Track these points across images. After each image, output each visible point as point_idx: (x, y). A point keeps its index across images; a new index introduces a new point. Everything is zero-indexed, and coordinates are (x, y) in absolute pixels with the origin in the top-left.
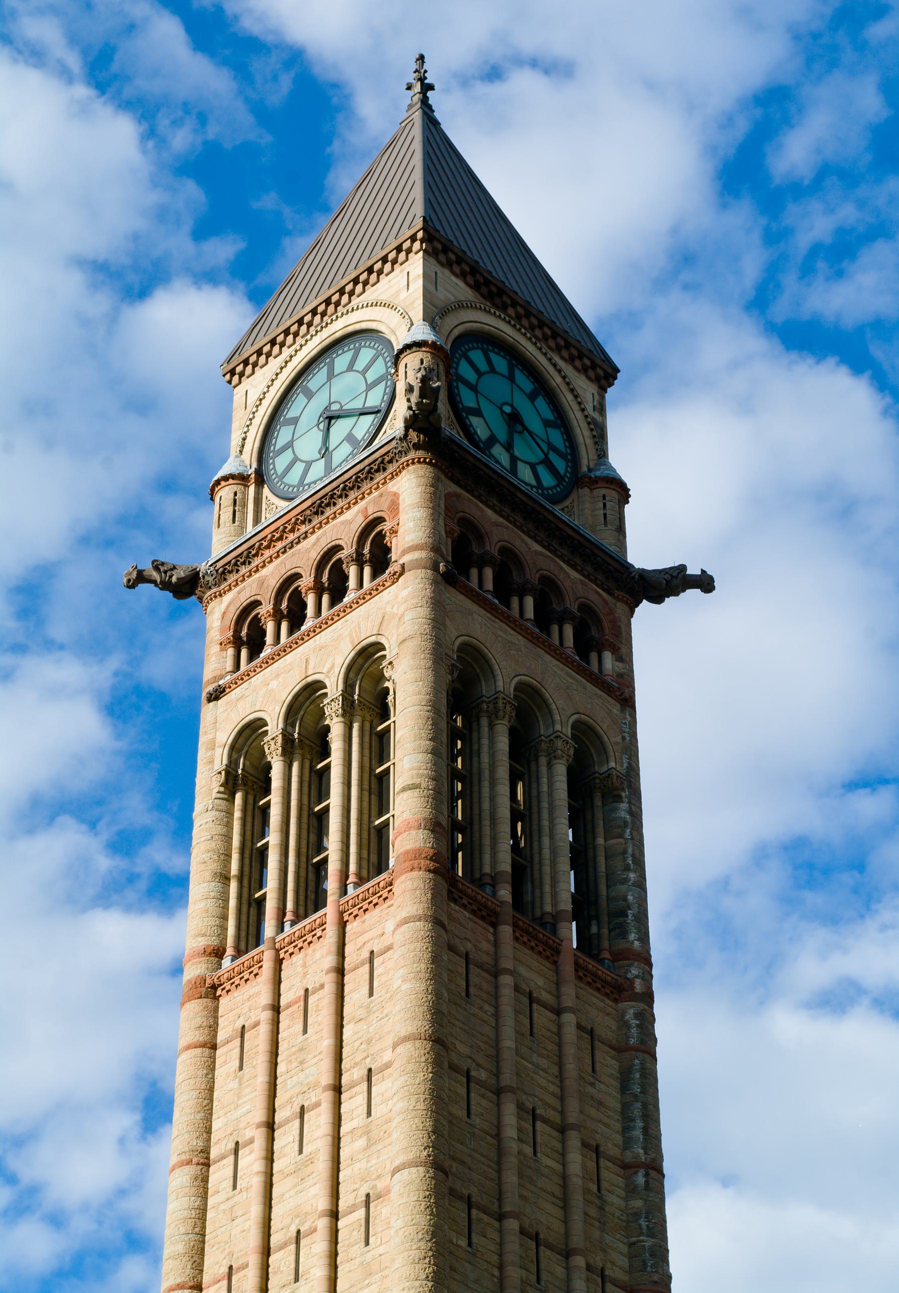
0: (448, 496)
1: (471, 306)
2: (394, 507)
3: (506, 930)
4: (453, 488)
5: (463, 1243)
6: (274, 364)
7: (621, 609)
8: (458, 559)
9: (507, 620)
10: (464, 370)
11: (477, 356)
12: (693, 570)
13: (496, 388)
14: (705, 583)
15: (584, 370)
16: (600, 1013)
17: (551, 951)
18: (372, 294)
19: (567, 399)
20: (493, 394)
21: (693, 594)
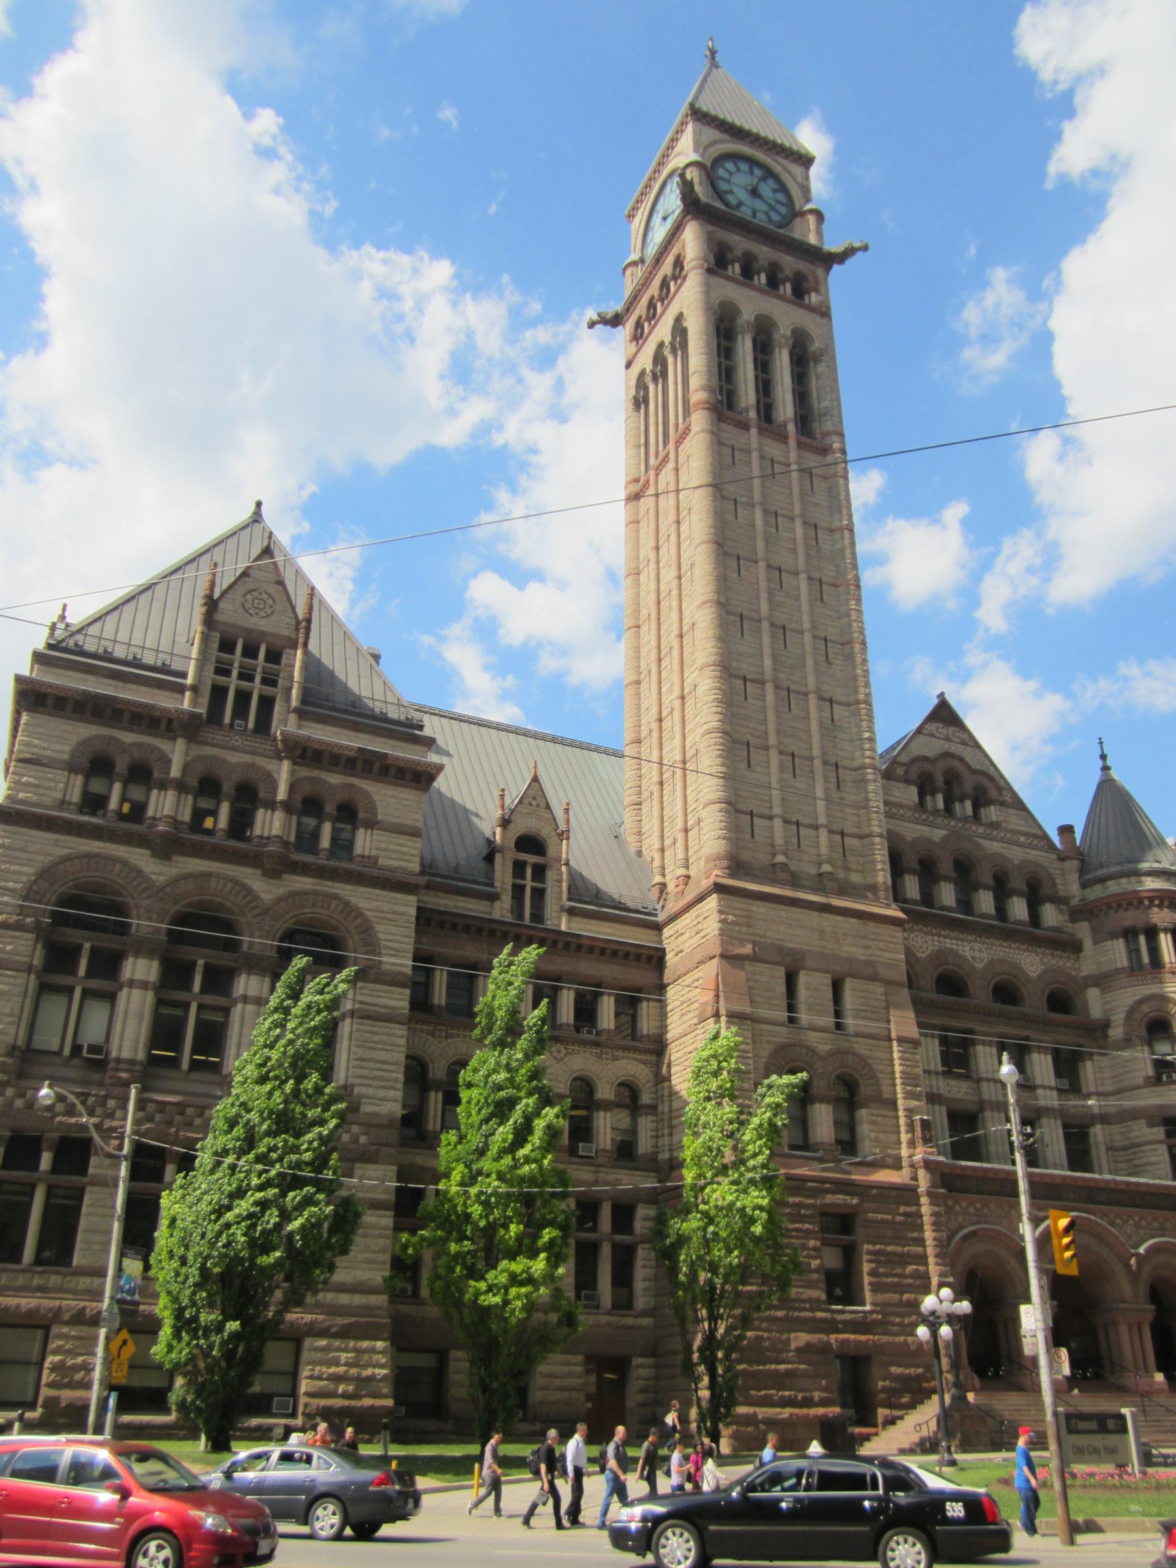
0: (709, 233)
1: (723, 141)
2: (684, 247)
3: (754, 431)
4: (711, 228)
5: (735, 575)
7: (820, 272)
9: (754, 288)
10: (721, 172)
11: (730, 166)
12: (857, 245)
14: (865, 248)
15: (795, 161)
18: (675, 151)
19: (785, 177)
20: (738, 182)
21: (859, 254)
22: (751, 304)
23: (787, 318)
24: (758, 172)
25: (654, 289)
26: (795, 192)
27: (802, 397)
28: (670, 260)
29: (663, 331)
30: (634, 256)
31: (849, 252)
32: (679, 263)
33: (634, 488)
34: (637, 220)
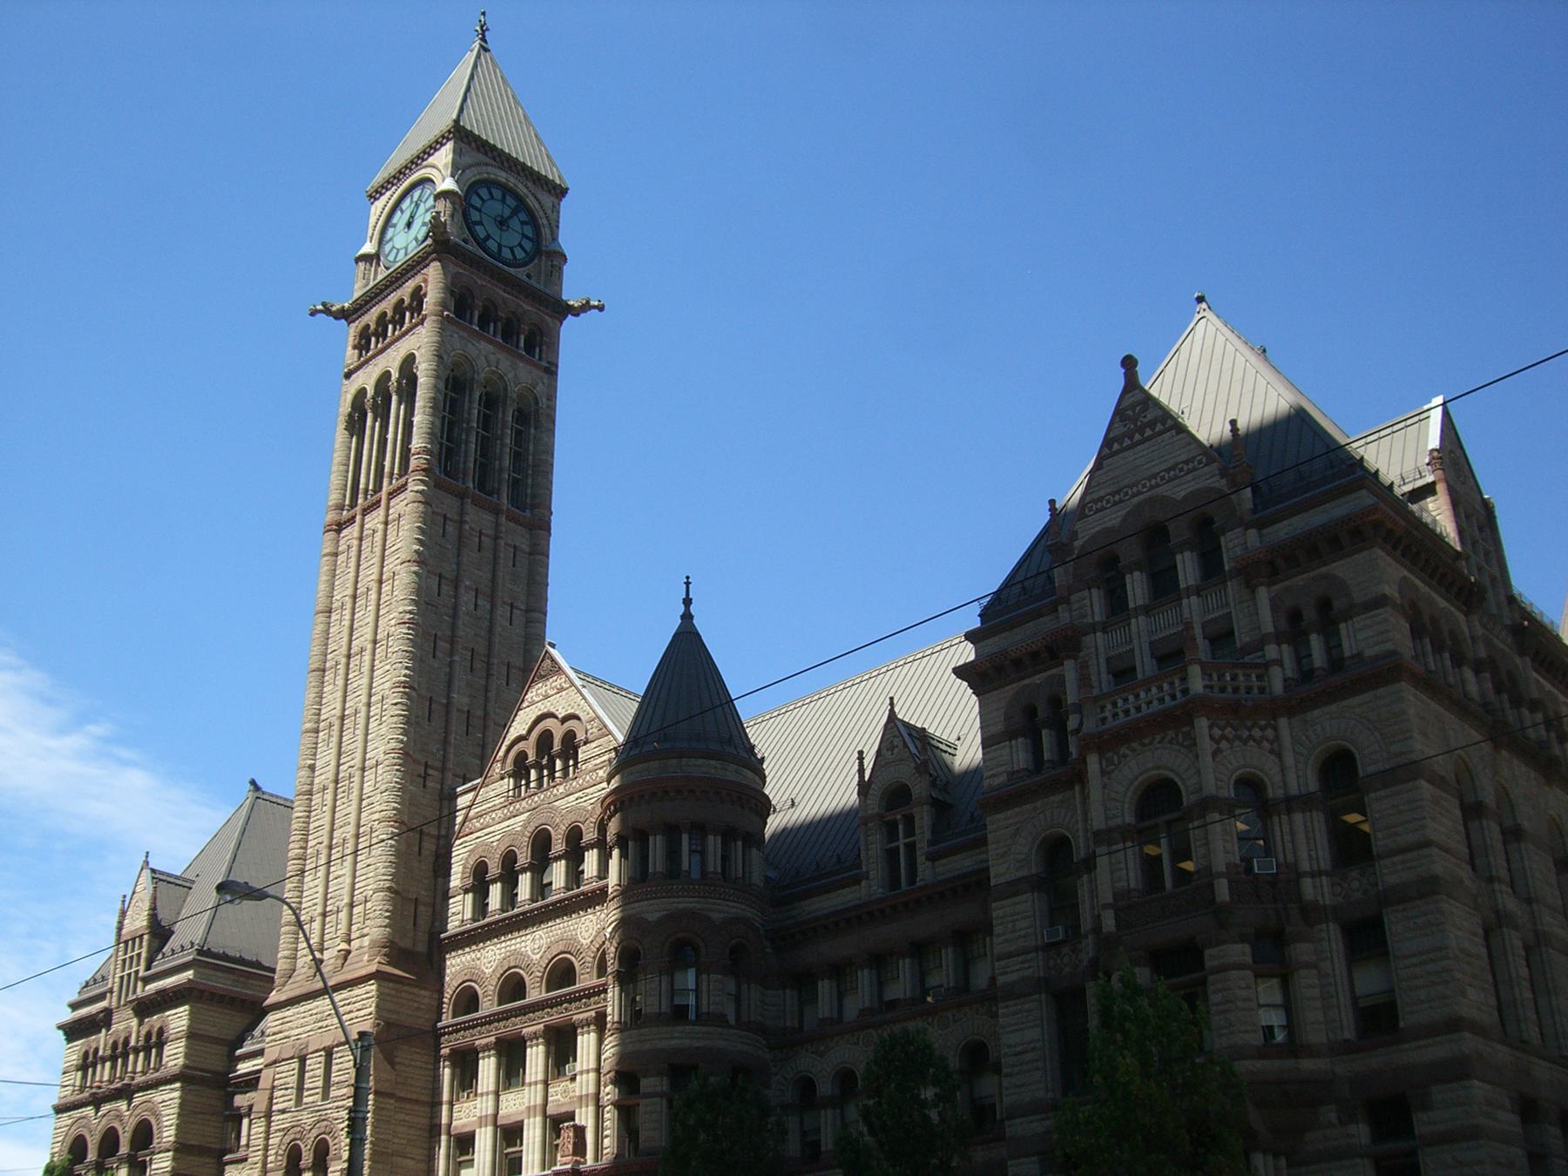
0: (456, 276)
2: (425, 281)
6: (388, 194)
8: (461, 306)
10: (476, 201)
11: (484, 192)
13: (495, 208)
14: (601, 308)
16: (521, 539)
17: (497, 512)
18: (431, 160)
22: (487, 357)
23: (518, 374)
24: (510, 201)
25: (387, 305)
26: (546, 232)
27: (518, 457)
28: (410, 286)
29: (390, 361)
30: (369, 248)
31: (586, 307)
32: (418, 296)
33: (331, 516)
34: (380, 203)
